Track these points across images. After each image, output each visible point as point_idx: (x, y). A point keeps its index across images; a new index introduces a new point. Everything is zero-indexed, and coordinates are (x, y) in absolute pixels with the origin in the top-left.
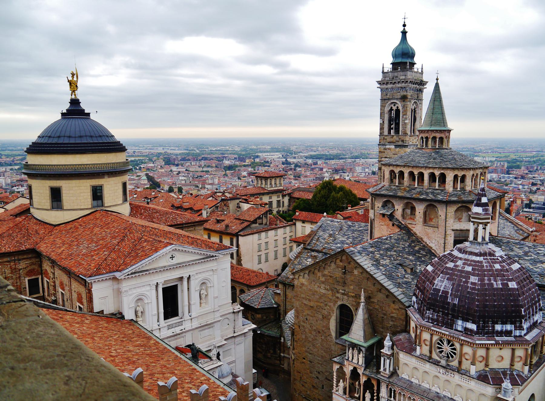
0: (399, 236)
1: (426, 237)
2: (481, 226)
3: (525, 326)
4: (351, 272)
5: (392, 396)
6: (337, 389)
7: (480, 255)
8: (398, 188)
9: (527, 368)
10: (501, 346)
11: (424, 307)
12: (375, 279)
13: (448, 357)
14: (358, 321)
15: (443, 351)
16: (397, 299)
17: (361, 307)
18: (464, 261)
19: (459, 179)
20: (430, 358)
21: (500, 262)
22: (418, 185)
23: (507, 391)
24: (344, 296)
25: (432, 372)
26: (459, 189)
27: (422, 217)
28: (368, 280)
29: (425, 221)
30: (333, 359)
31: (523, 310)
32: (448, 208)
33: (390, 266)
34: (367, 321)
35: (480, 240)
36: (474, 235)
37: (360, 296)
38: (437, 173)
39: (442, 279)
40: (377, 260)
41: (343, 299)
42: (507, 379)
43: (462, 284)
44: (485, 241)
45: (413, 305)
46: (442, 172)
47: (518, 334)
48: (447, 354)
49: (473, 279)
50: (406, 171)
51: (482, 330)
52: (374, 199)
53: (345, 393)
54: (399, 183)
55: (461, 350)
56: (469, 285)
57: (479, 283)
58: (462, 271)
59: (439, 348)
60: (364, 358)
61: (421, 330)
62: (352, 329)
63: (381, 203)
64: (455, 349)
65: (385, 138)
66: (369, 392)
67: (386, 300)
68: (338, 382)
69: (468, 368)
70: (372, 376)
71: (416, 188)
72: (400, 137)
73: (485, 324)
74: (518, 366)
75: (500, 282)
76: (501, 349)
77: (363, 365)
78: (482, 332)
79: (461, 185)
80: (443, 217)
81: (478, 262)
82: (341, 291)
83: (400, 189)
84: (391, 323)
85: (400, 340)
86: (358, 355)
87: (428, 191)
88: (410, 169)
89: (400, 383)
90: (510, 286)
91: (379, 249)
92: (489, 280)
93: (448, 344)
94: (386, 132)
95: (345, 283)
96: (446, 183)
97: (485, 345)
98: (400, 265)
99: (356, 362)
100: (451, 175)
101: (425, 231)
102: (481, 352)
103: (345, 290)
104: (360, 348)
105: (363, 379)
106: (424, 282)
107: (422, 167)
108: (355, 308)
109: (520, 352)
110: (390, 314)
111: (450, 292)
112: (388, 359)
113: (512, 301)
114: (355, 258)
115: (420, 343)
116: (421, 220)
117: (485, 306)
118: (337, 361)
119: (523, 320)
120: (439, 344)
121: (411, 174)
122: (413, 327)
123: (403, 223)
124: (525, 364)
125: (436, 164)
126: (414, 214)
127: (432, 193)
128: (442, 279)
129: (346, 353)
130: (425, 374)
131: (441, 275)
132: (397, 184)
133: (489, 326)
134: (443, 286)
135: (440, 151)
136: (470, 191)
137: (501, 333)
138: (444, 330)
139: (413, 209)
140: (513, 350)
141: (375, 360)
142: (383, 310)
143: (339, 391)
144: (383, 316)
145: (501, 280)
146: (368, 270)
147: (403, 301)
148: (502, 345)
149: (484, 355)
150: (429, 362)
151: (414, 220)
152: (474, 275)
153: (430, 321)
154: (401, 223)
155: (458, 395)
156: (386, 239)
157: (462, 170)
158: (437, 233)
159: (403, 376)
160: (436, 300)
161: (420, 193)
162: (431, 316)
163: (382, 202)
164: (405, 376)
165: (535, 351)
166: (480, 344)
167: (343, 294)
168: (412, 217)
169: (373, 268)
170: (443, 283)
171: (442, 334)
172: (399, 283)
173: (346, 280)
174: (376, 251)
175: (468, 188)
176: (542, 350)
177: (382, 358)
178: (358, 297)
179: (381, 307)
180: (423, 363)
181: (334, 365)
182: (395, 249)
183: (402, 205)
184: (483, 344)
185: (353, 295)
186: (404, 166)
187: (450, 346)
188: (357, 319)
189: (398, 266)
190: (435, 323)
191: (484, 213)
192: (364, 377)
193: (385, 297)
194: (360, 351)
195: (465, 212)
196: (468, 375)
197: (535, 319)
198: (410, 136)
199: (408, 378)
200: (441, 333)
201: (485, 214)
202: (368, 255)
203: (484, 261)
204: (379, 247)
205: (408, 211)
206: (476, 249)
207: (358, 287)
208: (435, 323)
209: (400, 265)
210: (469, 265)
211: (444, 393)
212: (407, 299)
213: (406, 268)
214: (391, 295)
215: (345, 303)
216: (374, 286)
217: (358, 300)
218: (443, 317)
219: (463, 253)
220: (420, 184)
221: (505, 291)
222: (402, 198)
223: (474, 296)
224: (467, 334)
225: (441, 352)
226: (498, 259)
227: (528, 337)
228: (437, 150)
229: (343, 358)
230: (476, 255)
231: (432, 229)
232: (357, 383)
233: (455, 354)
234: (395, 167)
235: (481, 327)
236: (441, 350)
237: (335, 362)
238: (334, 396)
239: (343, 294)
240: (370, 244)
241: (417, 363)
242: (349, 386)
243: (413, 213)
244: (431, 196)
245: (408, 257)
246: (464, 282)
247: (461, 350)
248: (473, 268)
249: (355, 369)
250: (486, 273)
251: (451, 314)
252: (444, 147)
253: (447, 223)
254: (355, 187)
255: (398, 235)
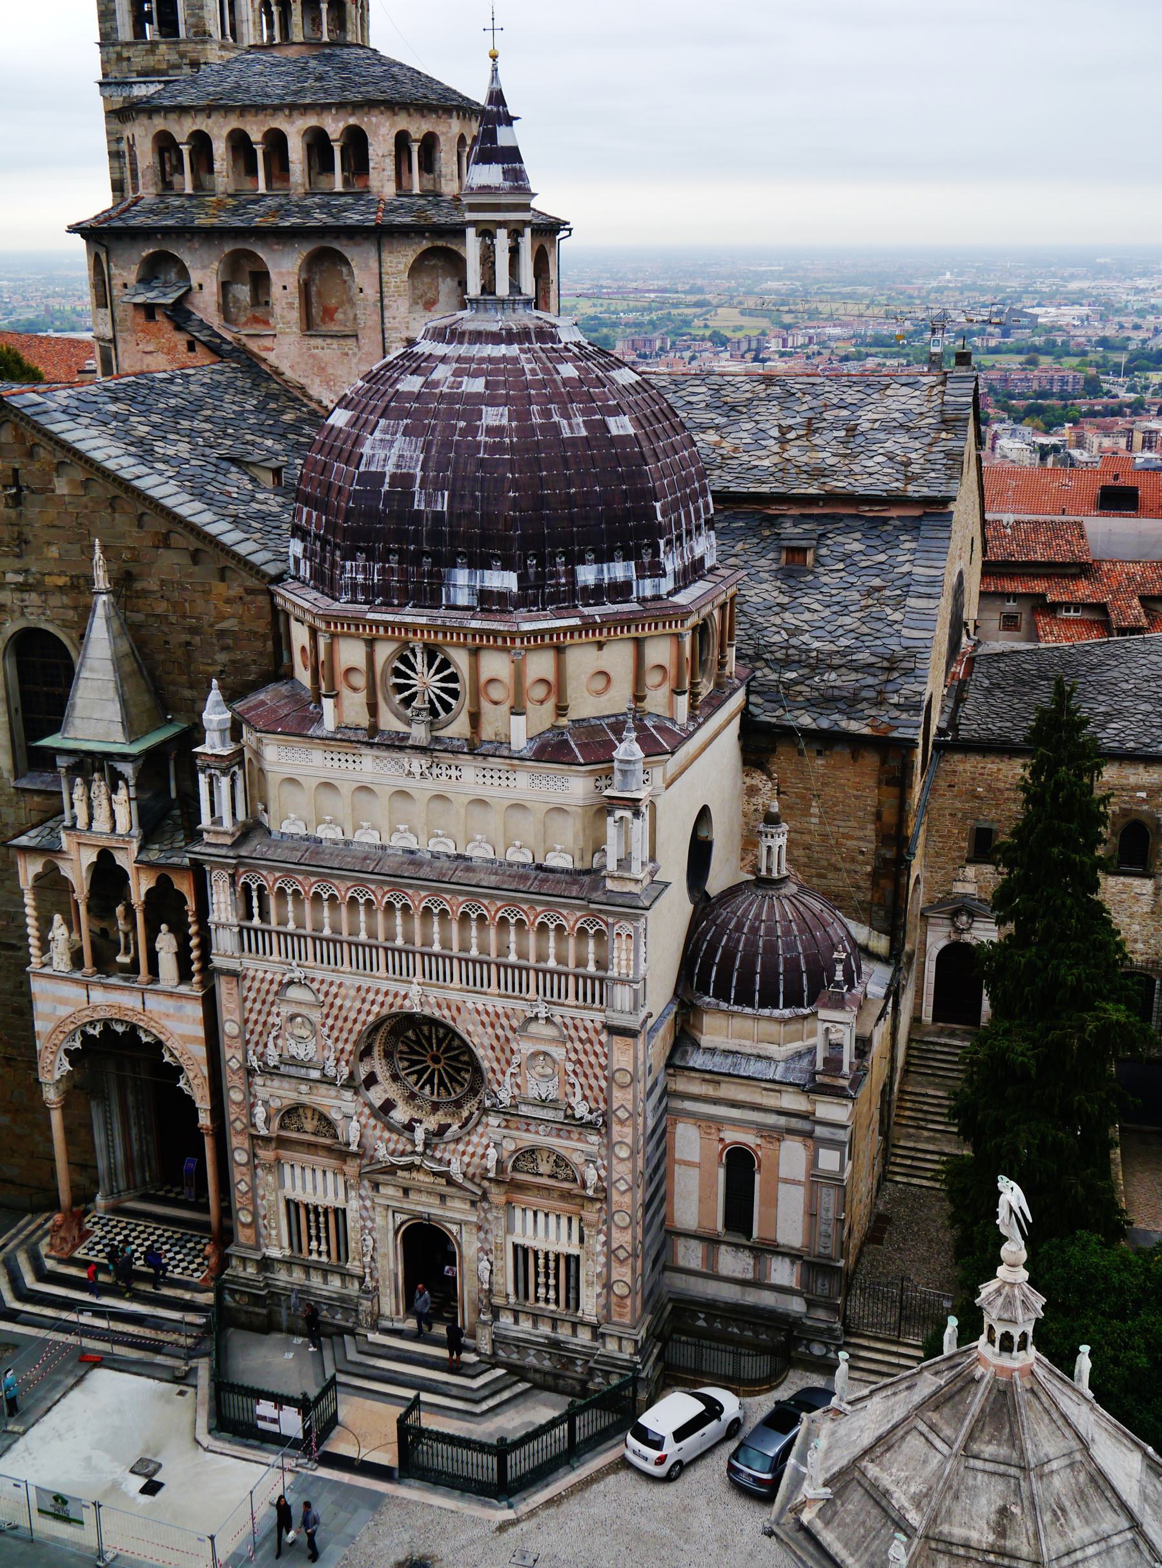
0: (217, 377)
1: (317, 381)
2: (502, 235)
3: (671, 563)
4: (43, 491)
5: (256, 911)
6: (45, 959)
7: (509, 337)
8: (195, 202)
9: (683, 701)
10: (601, 633)
11: (333, 554)
12: (141, 496)
13: (434, 712)
14: (92, 670)
15: (413, 696)
16: (235, 556)
17: (100, 611)
18: (455, 365)
19: (415, 148)
20: (374, 729)
21: (576, 358)
22: (269, 185)
23: (631, 767)
24: (26, 596)
25: (384, 781)
26: (416, 190)
27: (297, 305)
28: (114, 510)
29: (308, 325)
30: (15, 842)
31: (658, 505)
32: (384, 255)
33: (193, 462)
34: (128, 665)
35: (502, 288)
36: (483, 275)
37: (90, 581)
38: (334, 127)
39: (388, 437)
40: (141, 442)
41: (23, 608)
42: (629, 730)
43: (456, 438)
44: (520, 294)
45: (293, 572)
46: (352, 121)
47: (649, 593)
48: (431, 701)
49: (493, 416)
50: (219, 130)
51: (537, 587)
52: (103, 257)
53: (77, 960)
54: (198, 185)
55: (475, 670)
56: (482, 438)
57: (514, 424)
58: (451, 398)
59: (400, 688)
60: (134, 804)
61: (334, 636)
62: (73, 706)
63: (135, 268)
64: (453, 678)
65: (125, 54)
66: (170, 931)
67: (190, 575)
68: (45, 924)
69: (502, 731)
70: (170, 861)
71: (263, 195)
72: (182, 47)
73: (544, 568)
74: (657, 700)
75: (580, 420)
76: (600, 645)
77: (136, 831)
78: (536, 597)
79: (425, 182)
80: (371, 293)
81: (504, 359)
82: (10, 577)
83: (202, 206)
84: (222, 657)
85: (263, 703)
86: (110, 800)
87: (308, 202)
88: (233, 123)
89: (278, 854)
90: (615, 431)
91: (144, 408)
92: (546, 414)
93: (430, 667)
94: (125, 33)
95: (22, 540)
96: (371, 164)
97: (551, 638)
98: (233, 461)
99: (107, 828)
100: (383, 130)
101: (313, 356)
102: (540, 665)
103: (27, 571)
104: (113, 770)
105: (140, 886)
106: (325, 468)
107: (277, 109)
108: (75, 635)
109: (659, 652)
110: (211, 626)
111: (419, 473)
112: (224, 774)
113: (622, 478)
114: (54, 428)
115: (332, 686)
116: (295, 315)
117: (541, 502)
118: (32, 843)
119: (662, 542)
120: (398, 673)
121: (240, 143)
122: (303, 649)
123: (229, 338)
124: (677, 691)
125: (326, 91)
126: (267, 303)
127: (320, 206)
128: (388, 437)
129: (62, 812)
130: (363, 797)
131: (382, 422)
132: (189, 190)
133: (557, 572)
134: (393, 460)
135: (338, 52)
136: (456, 198)
137: (597, 594)
138: (411, 616)
139: (260, 280)
140: (639, 643)
141: (177, 812)
142: (184, 616)
143: (56, 960)
144: (186, 637)
145: (584, 412)
146: (111, 465)
147: (256, 559)
148: (605, 631)
149: (551, 677)
150: (371, 745)
151: (266, 323)
152: (492, 402)
153: (361, 598)
154: (220, 337)
155: (479, 837)
156: (171, 381)
157: (423, 116)
158: (355, 360)
159: (287, 828)
160: (372, 514)
161: (282, 211)
162: (360, 577)
163: (138, 260)
164: (292, 827)
165: (703, 663)
166: (535, 633)
167: (22, 588)
168: (260, 312)
169: (127, 461)
170: (391, 447)
171: (407, 631)
172: (236, 516)
173: (27, 530)
174: (131, 414)
175: (449, 188)
176: (723, 657)
177: (201, 777)
178: (82, 585)
179: (175, 605)
180: (351, 759)
181: (21, 863)
182: (209, 413)
183: (215, 265)
184: (542, 633)
185: (61, 581)
186: (209, 110)
187: (437, 672)
188: (88, 662)
189: (224, 465)
190: (378, 601)
191: (508, 184)
192: (142, 876)
193: (186, 560)
194: (114, 781)
195: (445, 277)
196: (506, 753)
197: (698, 552)
198: (223, 47)
199: (303, 832)
200: (401, 625)
201: (512, 188)
202: (105, 424)
203: (523, 356)
204: (142, 403)
205: (243, 292)
206: (493, 322)
207: (78, 547)
208: (378, 601)
209: (233, 461)
210: (475, 375)
211: (435, 846)
212: (268, 556)
213: (256, 471)
214: (209, 549)
215: (34, 620)
216: (140, 526)
217: (83, 600)
218: (404, 573)
219: (449, 343)
220: (276, 185)
221: (599, 448)
222: (211, 235)
223: (500, 470)
224: (490, 611)
225: (407, 702)
226: (567, 350)
227: (681, 599)
228: (327, 51)
229: (52, 829)
230: (495, 338)
231: (335, 343)
232: (120, 909)
233: (454, 694)
234: (172, 116)
235: (532, 577)
236: (406, 694)
237: (25, 850)
238: (37, 985)
239: (22, 588)
240: (106, 389)
241: (329, 763)
242: (93, 945)
243: (262, 300)
244: (320, 218)
245: (259, 440)
246: (464, 432)
247: (475, 670)
248: (487, 382)
249: (105, 855)
250: (533, 392)
251: (427, 554)
252: (350, 38)
253: (386, 314)
254: (33, 351)
255: (213, 372)
